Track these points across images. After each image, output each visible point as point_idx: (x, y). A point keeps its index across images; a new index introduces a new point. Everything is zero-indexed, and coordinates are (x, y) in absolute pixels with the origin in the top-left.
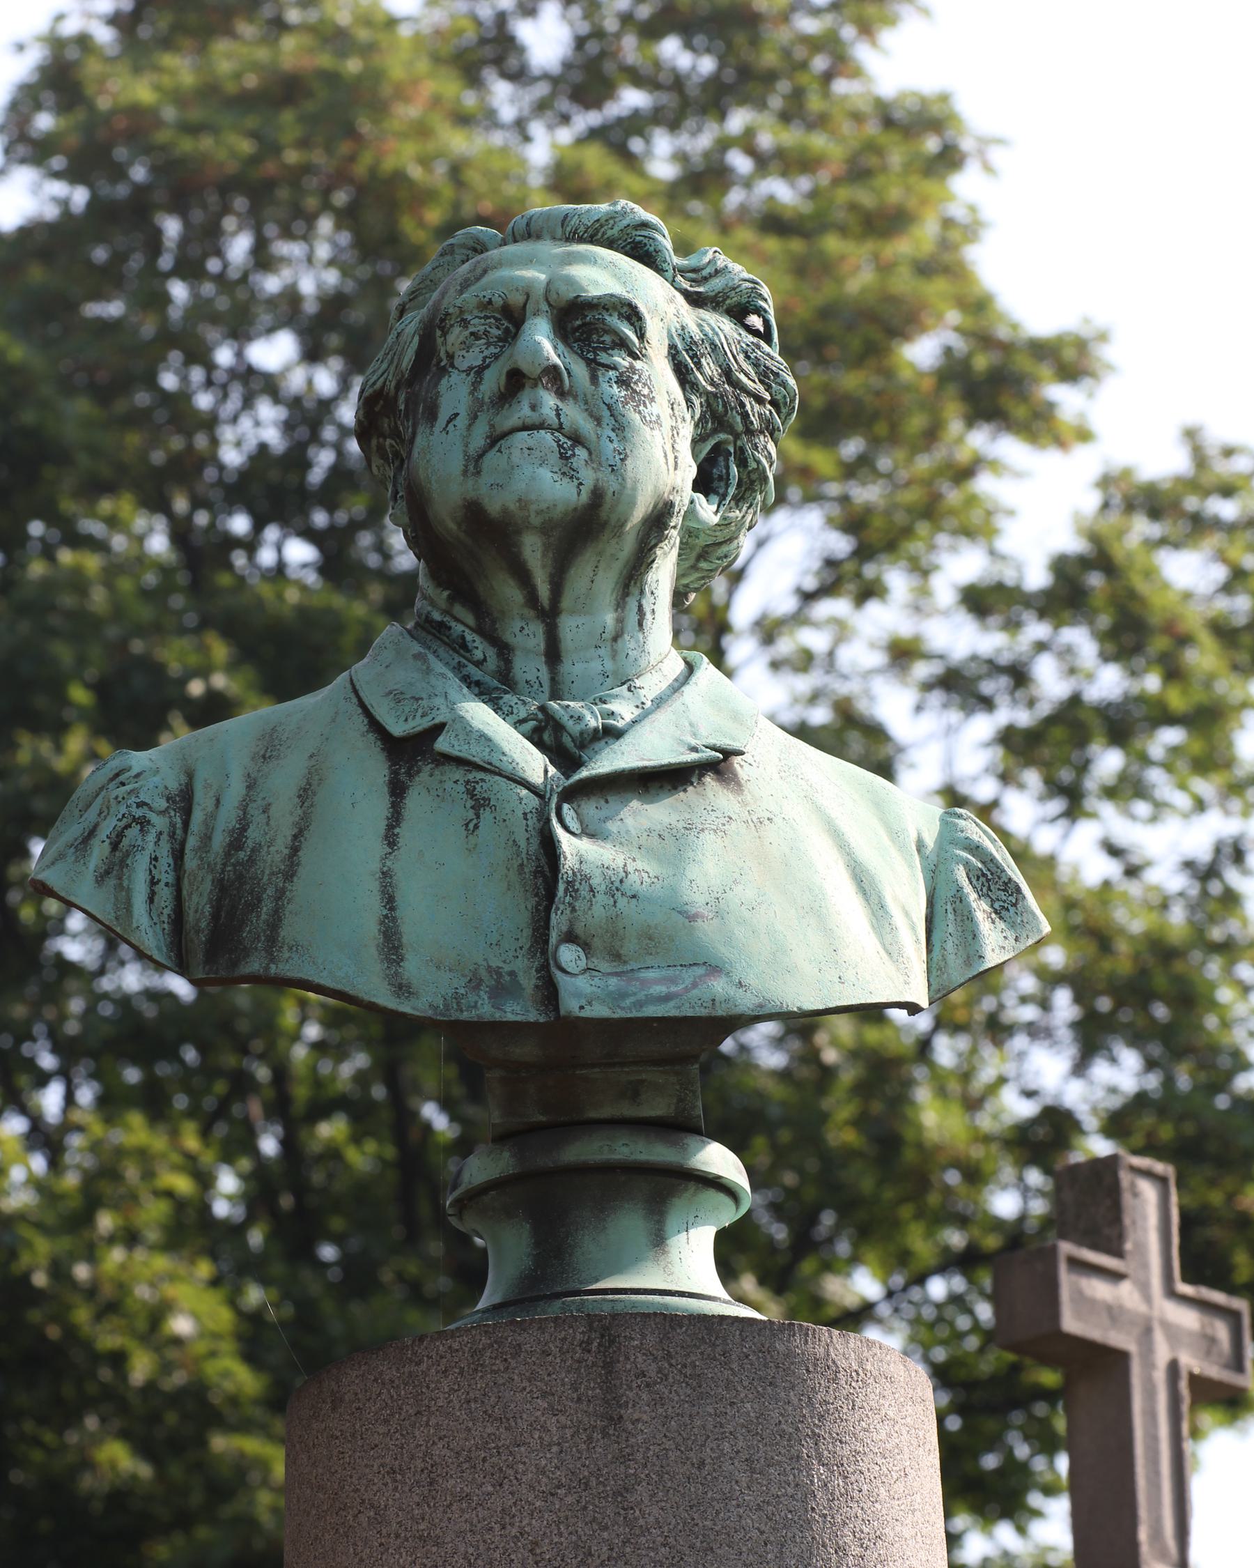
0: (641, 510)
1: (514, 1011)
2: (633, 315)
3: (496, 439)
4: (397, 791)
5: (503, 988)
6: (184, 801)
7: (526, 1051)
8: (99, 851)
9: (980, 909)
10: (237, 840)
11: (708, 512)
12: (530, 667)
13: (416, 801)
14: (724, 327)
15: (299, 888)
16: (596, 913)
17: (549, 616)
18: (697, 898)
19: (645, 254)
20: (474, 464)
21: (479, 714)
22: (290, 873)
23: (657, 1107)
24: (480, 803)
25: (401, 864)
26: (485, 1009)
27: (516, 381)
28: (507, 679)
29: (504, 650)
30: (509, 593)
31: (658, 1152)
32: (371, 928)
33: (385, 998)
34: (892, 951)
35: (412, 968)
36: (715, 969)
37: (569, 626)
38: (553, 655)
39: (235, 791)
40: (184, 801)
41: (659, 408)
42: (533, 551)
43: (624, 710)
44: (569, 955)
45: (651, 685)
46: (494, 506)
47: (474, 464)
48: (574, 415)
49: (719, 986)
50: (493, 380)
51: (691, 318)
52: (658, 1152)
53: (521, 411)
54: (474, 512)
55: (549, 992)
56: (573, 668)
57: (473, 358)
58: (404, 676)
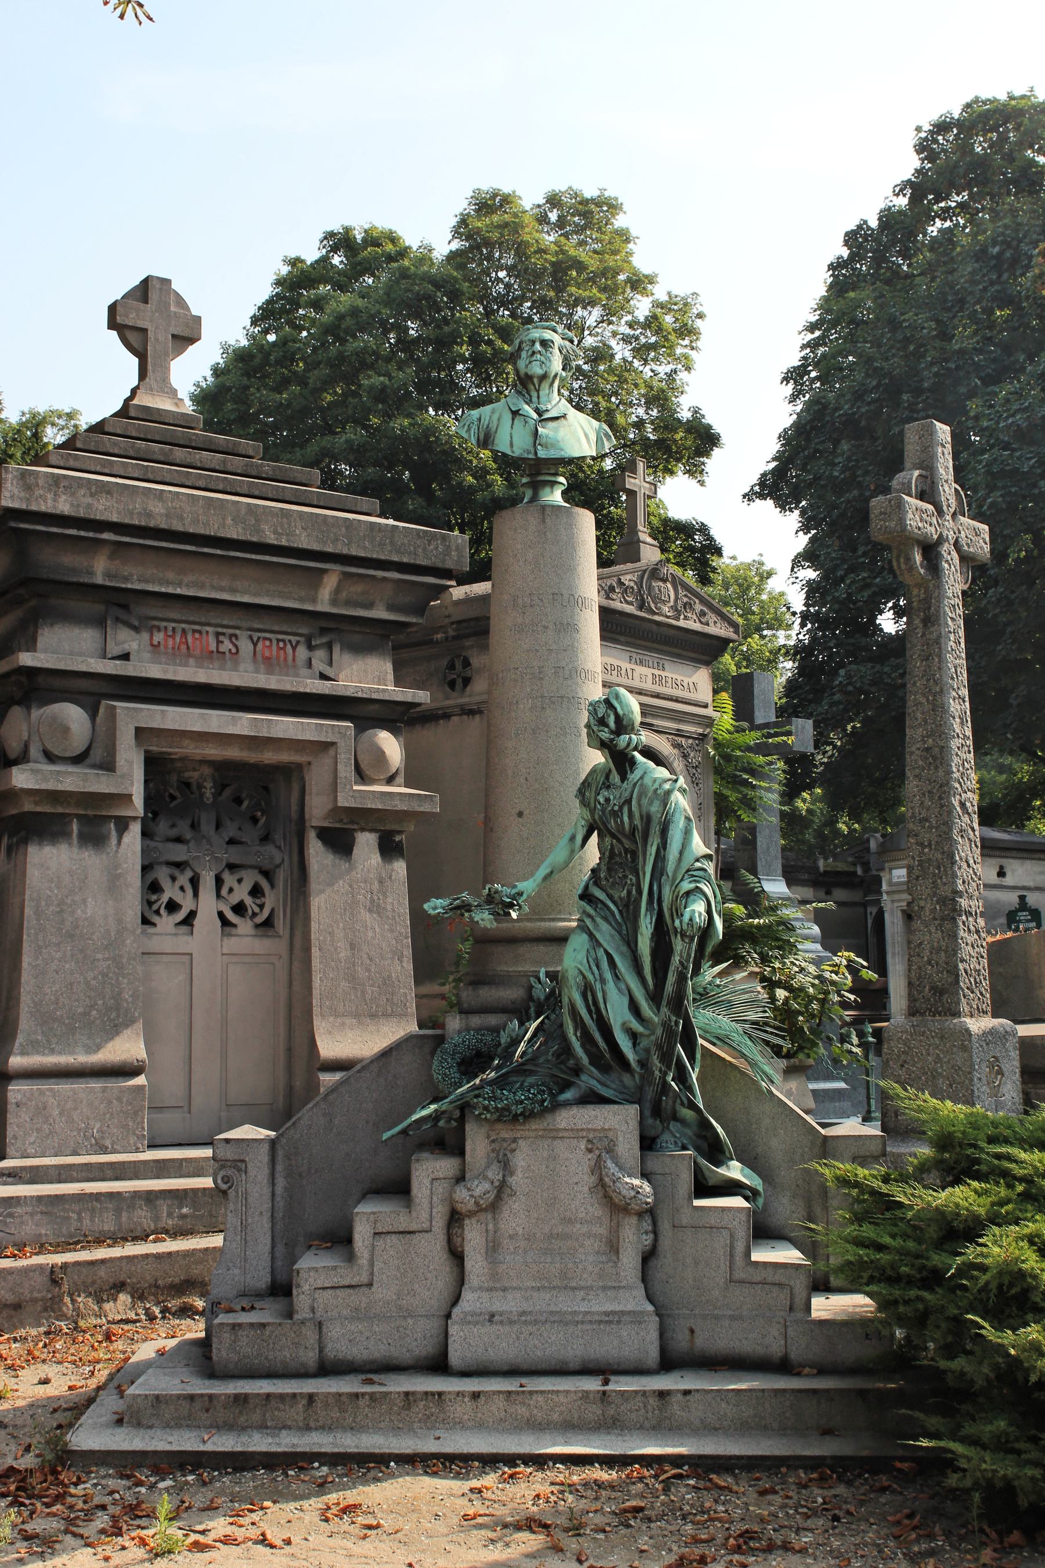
0: (553, 374)
1: (531, 456)
2: (553, 342)
3: (530, 362)
4: (513, 420)
5: (529, 452)
6: (479, 420)
7: (532, 462)
8: (466, 427)
9: (605, 439)
10: (488, 426)
11: (564, 374)
12: (535, 399)
13: (516, 421)
14: (567, 343)
15: (497, 435)
16: (544, 441)
17: (538, 391)
18: (559, 439)
19: (555, 331)
20: (527, 366)
21: (526, 407)
22: (496, 432)
23: (552, 471)
24: (526, 422)
25: (514, 432)
26: (526, 456)
27: (534, 353)
28: (531, 401)
29: (531, 397)
30: (532, 387)
31: (552, 479)
32: (508, 442)
33: (510, 453)
34: (590, 446)
35: (515, 449)
36: (562, 450)
37: (541, 393)
38: (538, 397)
39: (488, 418)
40: (479, 420)
41: (556, 357)
42: (536, 381)
43: (549, 407)
44: (539, 447)
45: (554, 402)
46: (530, 373)
47: (527, 366)
48: (543, 359)
49: (563, 453)
50: (530, 352)
51: (562, 342)
52: (552, 479)
53: (534, 358)
54: (526, 374)
55: (536, 453)
56: (542, 399)
57: (527, 348)
58: (515, 400)
